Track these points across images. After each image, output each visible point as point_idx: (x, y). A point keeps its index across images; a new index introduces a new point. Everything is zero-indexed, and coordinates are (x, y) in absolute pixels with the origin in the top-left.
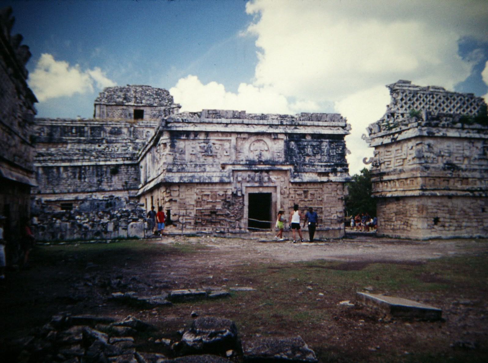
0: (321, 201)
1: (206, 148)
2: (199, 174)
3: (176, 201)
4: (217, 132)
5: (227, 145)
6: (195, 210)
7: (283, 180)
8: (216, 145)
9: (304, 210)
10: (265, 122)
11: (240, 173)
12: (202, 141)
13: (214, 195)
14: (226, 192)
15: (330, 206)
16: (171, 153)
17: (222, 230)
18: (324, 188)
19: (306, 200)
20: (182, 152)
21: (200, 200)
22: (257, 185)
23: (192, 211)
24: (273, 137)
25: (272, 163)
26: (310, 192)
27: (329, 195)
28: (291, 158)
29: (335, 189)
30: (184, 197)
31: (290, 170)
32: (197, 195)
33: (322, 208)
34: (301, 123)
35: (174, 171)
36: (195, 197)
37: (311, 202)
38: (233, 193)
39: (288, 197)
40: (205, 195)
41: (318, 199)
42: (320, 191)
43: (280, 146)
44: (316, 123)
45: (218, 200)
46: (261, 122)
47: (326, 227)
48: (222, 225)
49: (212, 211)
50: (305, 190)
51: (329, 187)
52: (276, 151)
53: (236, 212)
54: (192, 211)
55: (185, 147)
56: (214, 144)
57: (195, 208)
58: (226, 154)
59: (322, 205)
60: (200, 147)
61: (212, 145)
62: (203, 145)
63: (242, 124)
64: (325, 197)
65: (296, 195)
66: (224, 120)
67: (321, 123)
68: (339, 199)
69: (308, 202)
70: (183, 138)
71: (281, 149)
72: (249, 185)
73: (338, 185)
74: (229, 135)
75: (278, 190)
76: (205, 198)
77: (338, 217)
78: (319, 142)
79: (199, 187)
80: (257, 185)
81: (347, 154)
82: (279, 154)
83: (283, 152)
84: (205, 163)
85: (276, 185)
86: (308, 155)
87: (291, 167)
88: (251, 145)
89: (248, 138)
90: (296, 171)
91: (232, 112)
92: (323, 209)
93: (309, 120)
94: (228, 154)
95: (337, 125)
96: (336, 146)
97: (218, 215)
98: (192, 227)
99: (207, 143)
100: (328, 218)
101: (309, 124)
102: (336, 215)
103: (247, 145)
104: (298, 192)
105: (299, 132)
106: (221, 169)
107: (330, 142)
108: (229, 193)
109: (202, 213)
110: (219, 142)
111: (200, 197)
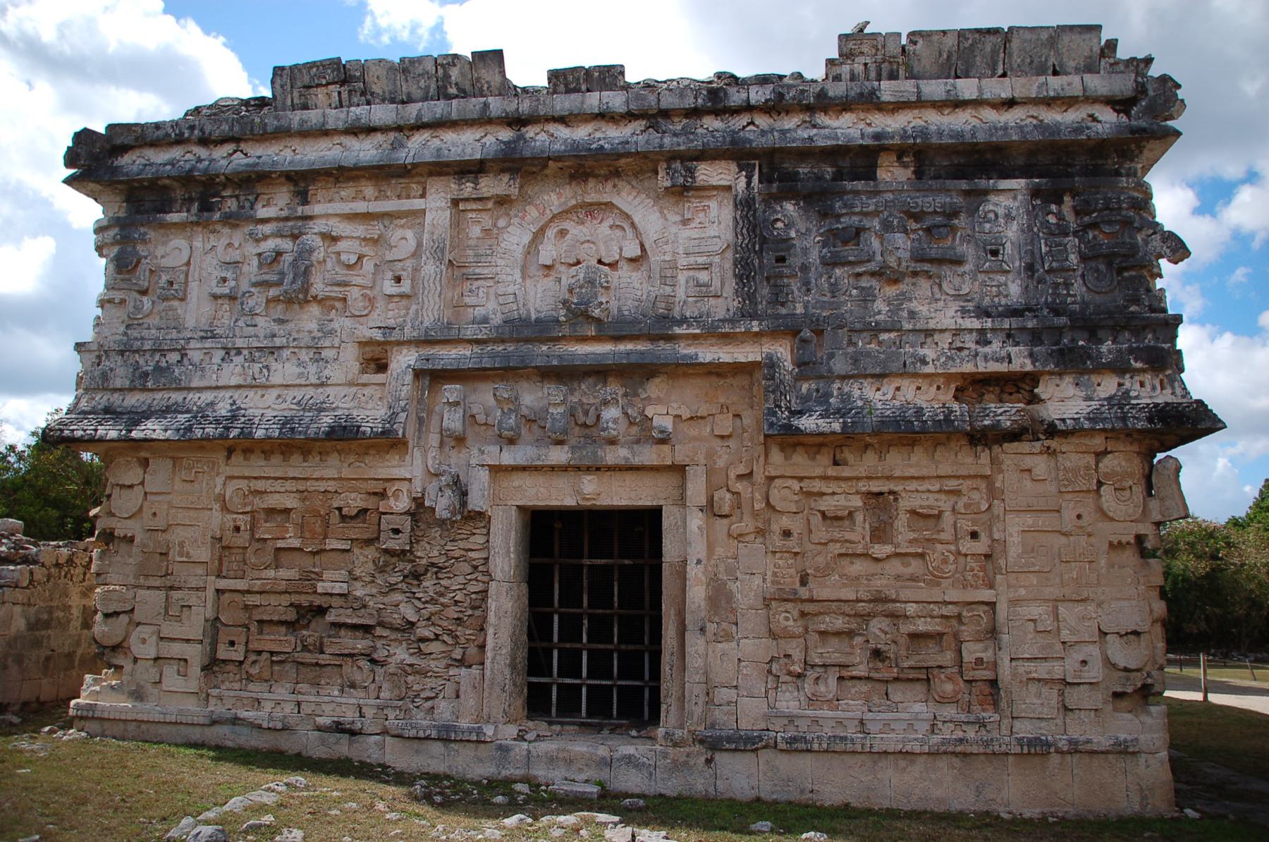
0: (987, 556)
1: (288, 258)
2: (237, 394)
3: (131, 540)
4: (340, 175)
5: (403, 240)
6: (210, 593)
7: (725, 424)
8: (342, 245)
9: (867, 617)
10: (616, 101)
11: (451, 391)
12: (267, 229)
13: (316, 514)
14: (382, 495)
15: (1052, 591)
16: (117, 296)
17: (349, 716)
18: (1008, 479)
19: (880, 550)
20: (175, 292)
21: (243, 539)
22: (559, 455)
23: (193, 599)
24: (664, 181)
25: (660, 326)
26: (905, 503)
27: (1043, 521)
28: (779, 297)
29: (1082, 484)
30: (160, 523)
31: (771, 364)
32: (225, 508)
33: (992, 605)
34: (836, 90)
35: (118, 383)
36: (216, 520)
37: (915, 567)
38: (419, 502)
39: (761, 532)
40: (271, 512)
41: (967, 546)
42: (979, 498)
43: (713, 231)
44: (935, 89)
45: (333, 544)
46: (593, 100)
47: (1025, 729)
48: (353, 686)
49: (304, 600)
50: (875, 487)
51: (1041, 465)
52: (683, 261)
53: (452, 612)
54: (193, 599)
55: (188, 264)
56: (330, 238)
57: (214, 583)
58: (389, 287)
59: (991, 586)
60: (260, 255)
61: (318, 241)
62: (270, 244)
63: (484, 120)
64: (1013, 530)
65: (817, 520)
66: (381, 113)
67: (967, 88)
68: (1116, 547)
69: (896, 567)
70: (174, 217)
71: (719, 245)
72: (508, 457)
73: (1099, 455)
74: (416, 188)
75: (697, 488)
76: (266, 530)
77: (1109, 664)
78: (967, 193)
79: (239, 465)
80: (559, 455)
81: (1163, 263)
82: (703, 276)
83: (726, 265)
84: (278, 342)
85: (680, 454)
86: (887, 275)
87: (783, 351)
88: (542, 231)
89: (525, 199)
90: (805, 367)
91: (430, 67)
92: (1002, 609)
93: (893, 76)
94: (406, 287)
95: (1077, 90)
96: (1077, 213)
97: (338, 626)
98: (193, 685)
99: (295, 237)
100: (1041, 670)
101: (886, 97)
102: (1094, 651)
103: (516, 237)
104: (827, 504)
105: (821, 143)
106: (355, 367)
107: (1035, 193)
108: (403, 504)
109: (246, 607)
110: (360, 230)
111: (243, 521)
